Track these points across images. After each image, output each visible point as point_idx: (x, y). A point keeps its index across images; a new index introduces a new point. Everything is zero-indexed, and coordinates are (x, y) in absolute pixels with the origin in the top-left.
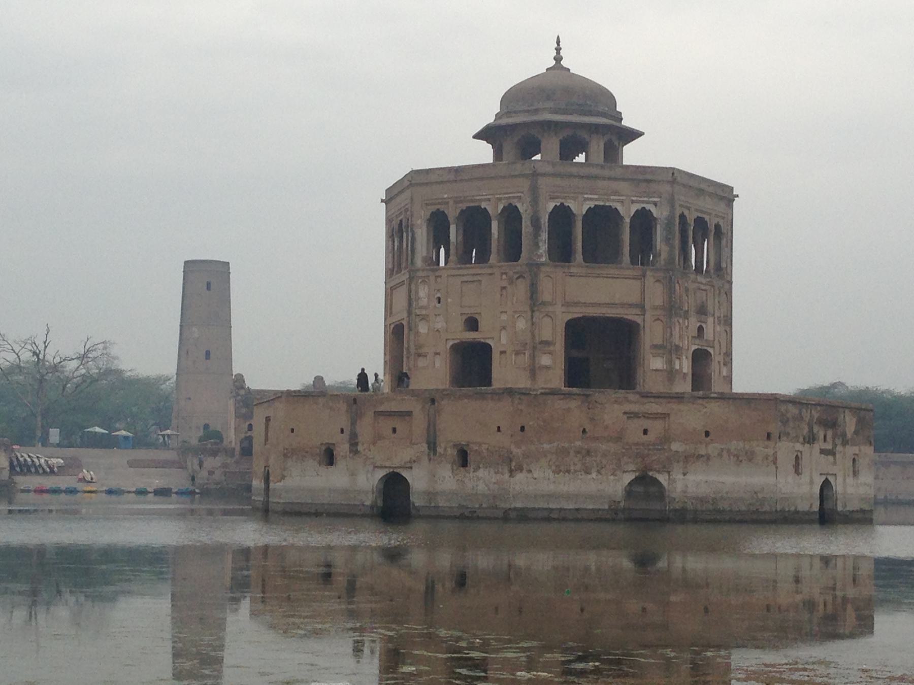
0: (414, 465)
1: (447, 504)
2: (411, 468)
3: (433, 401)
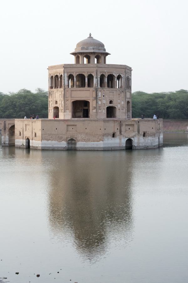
0: (135, 137)
1: (142, 145)
2: (134, 137)
3: (138, 122)
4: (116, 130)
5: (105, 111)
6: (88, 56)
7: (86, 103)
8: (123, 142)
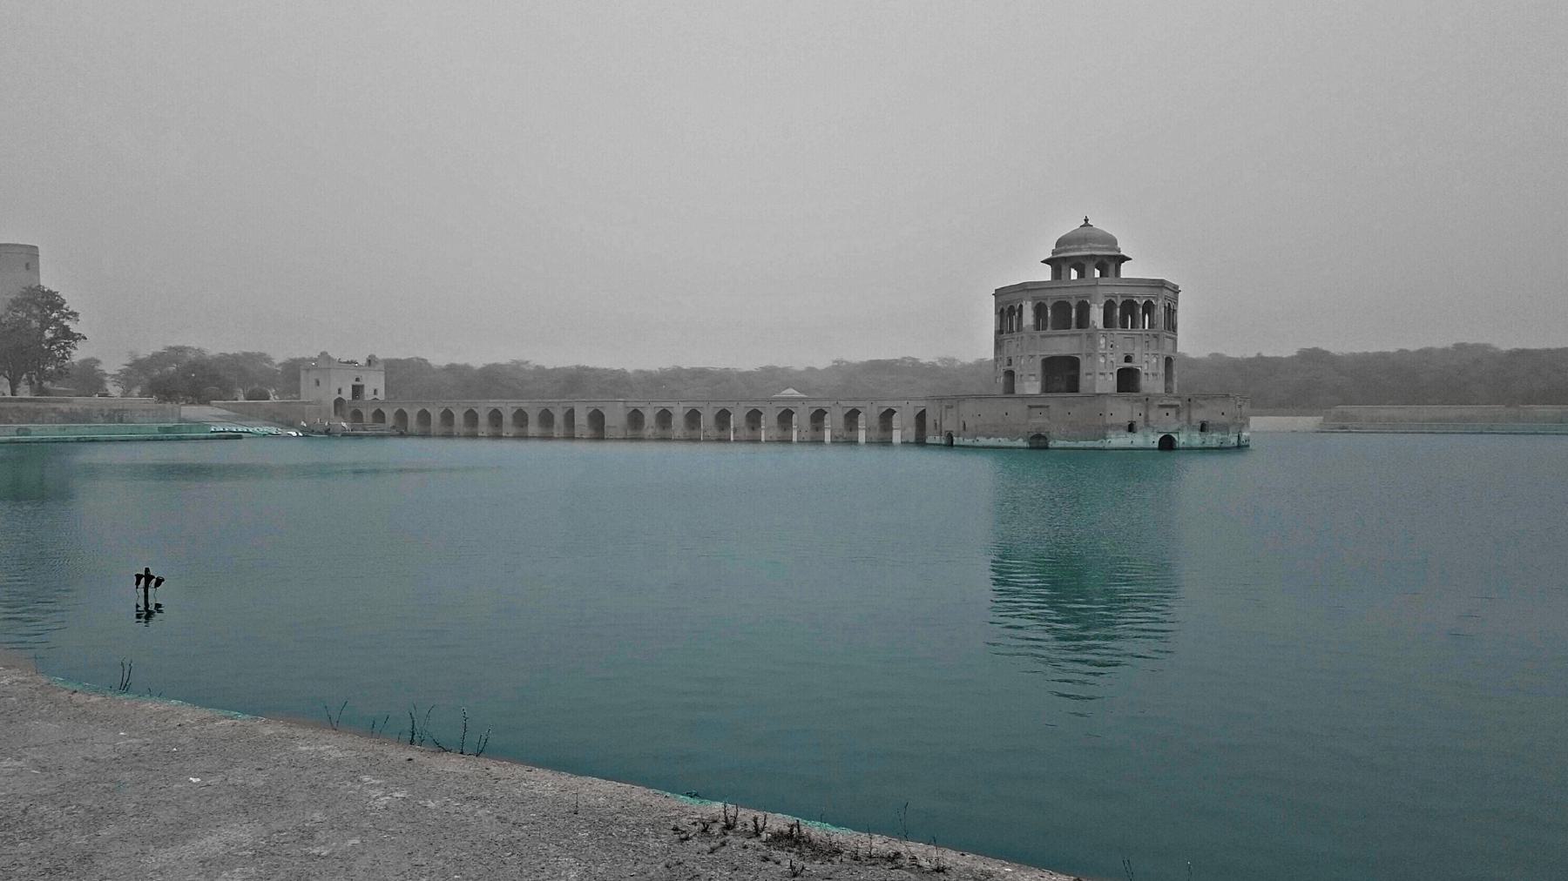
4: (1136, 418)
5: (1112, 380)
6: (1080, 264)
7: (1072, 363)
8: (1154, 440)
